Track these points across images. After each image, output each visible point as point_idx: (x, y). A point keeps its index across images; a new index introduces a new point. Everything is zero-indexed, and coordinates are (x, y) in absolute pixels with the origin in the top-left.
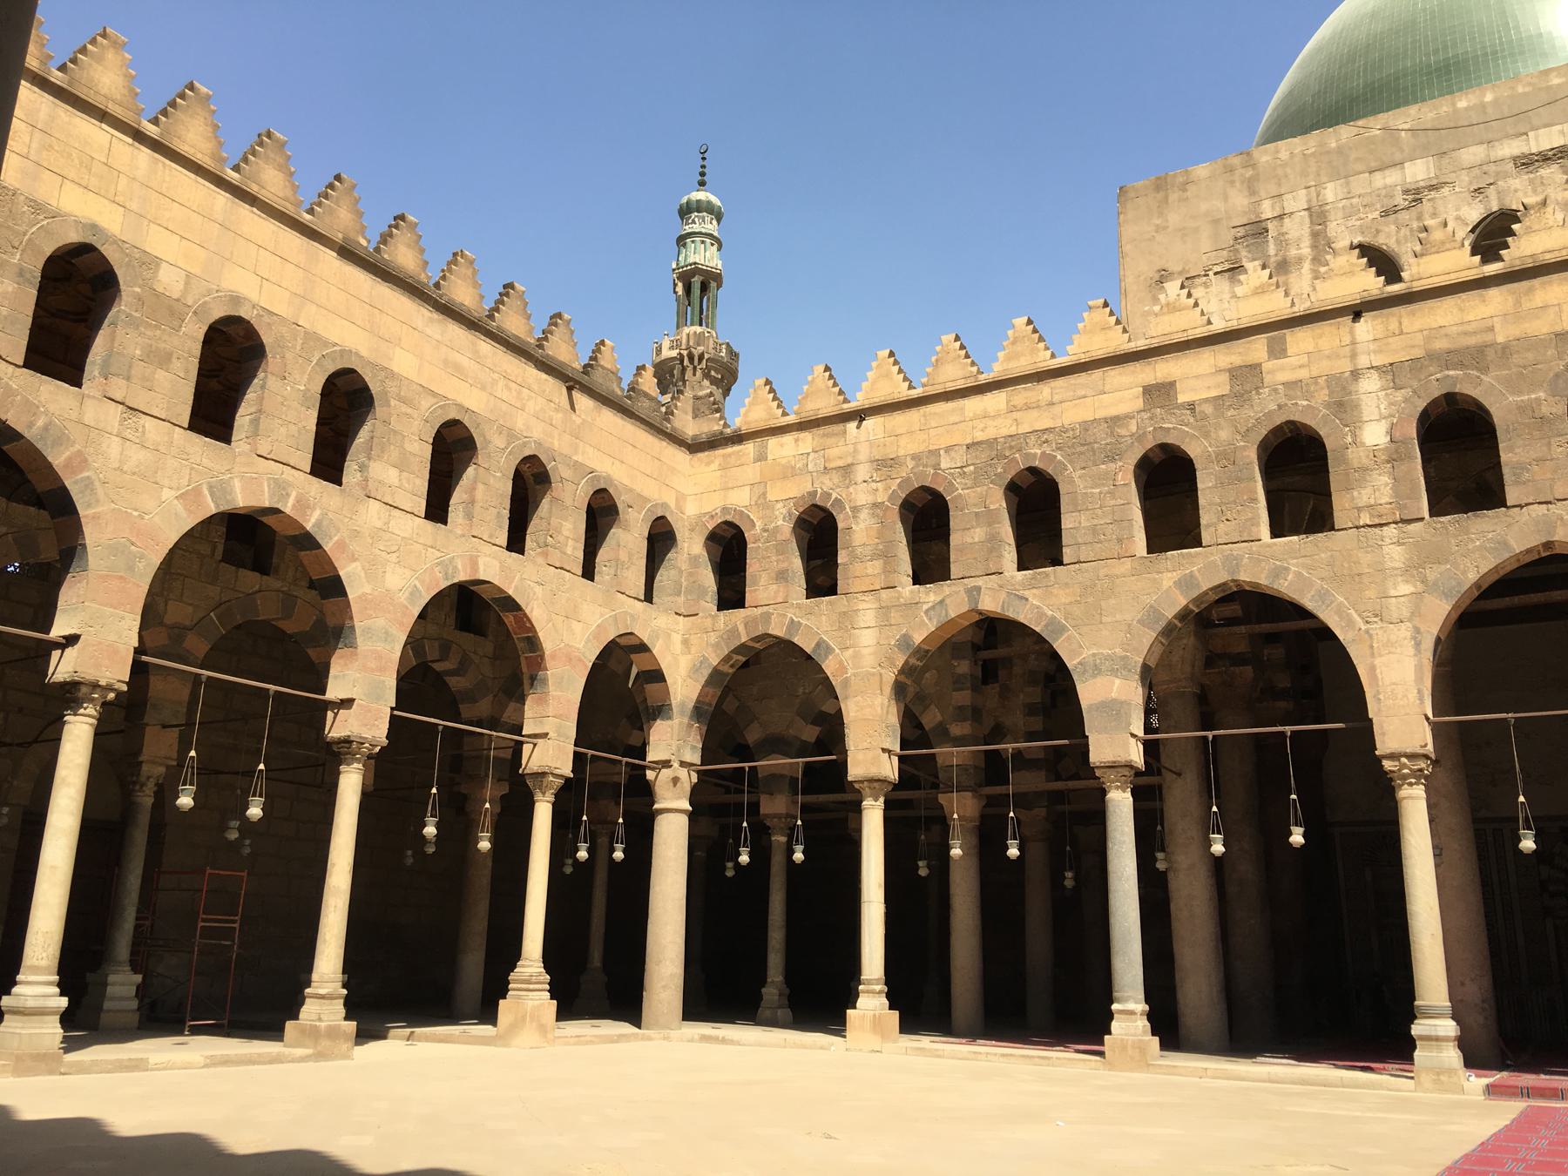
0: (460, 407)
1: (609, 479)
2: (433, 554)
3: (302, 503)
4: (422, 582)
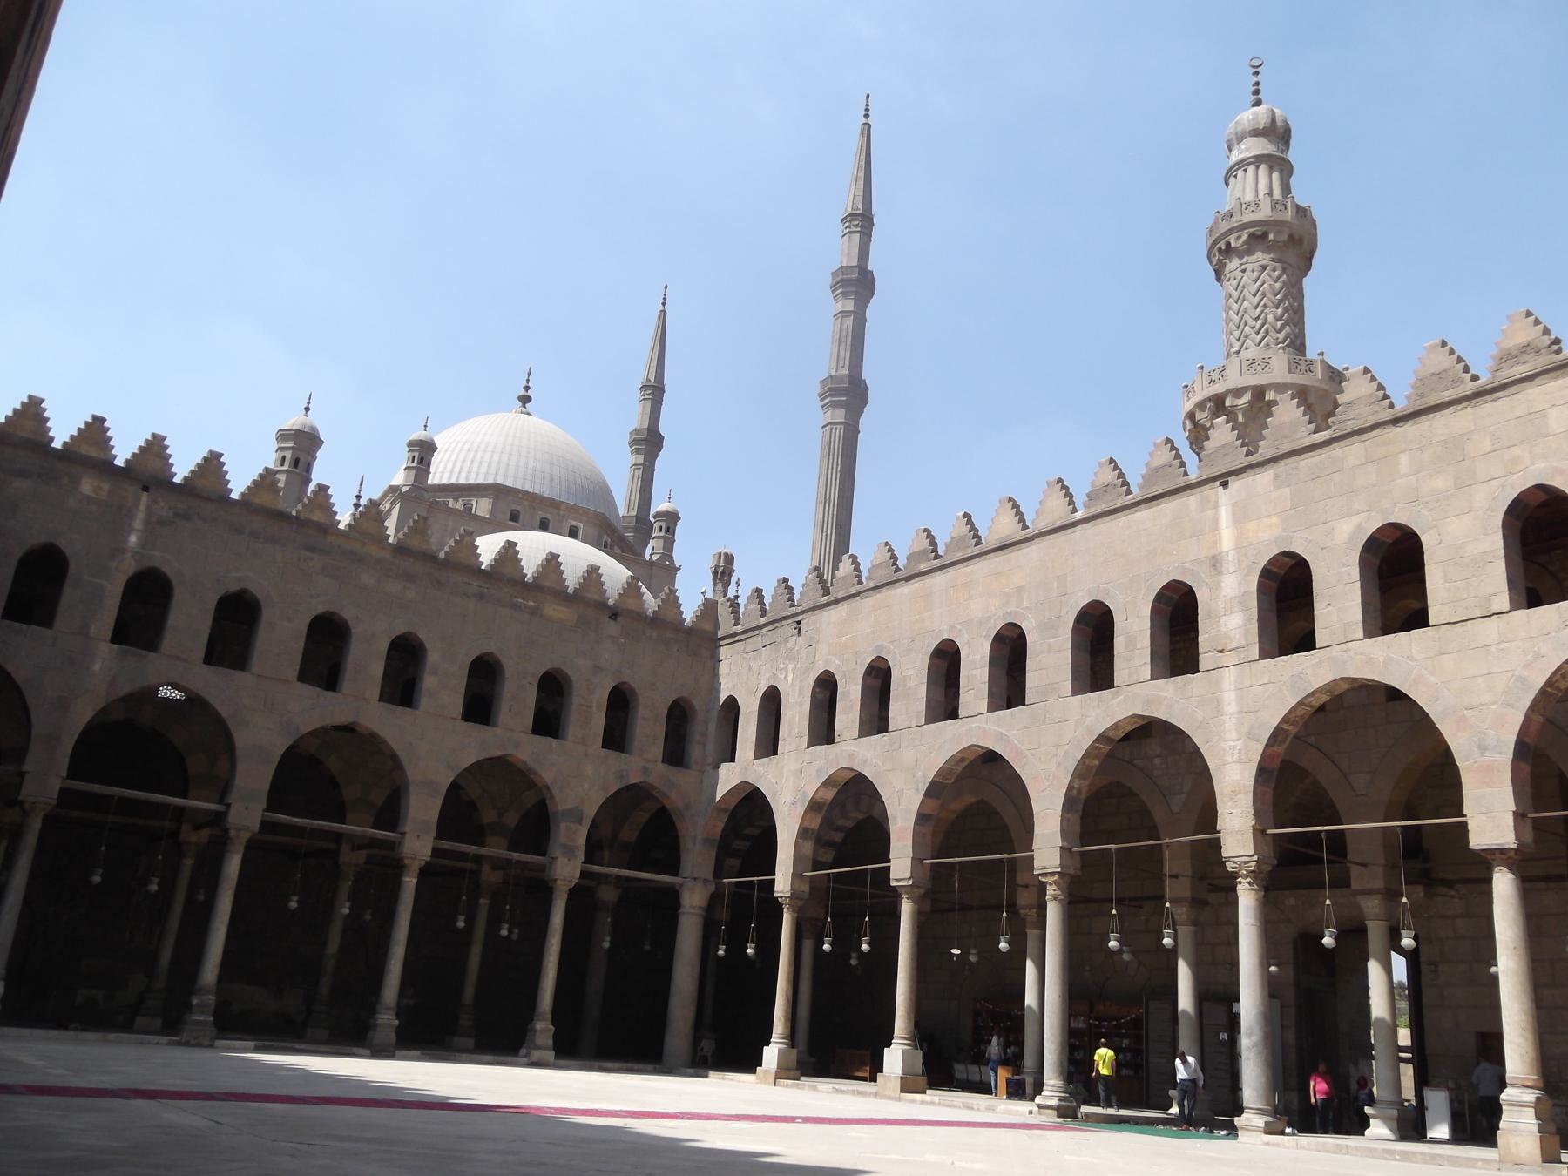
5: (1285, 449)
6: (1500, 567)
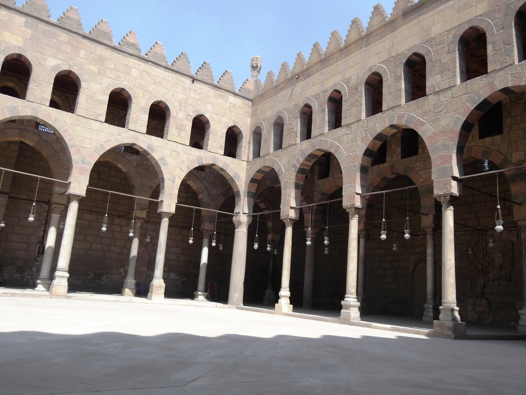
0: (467, 22)
3: (401, 117)
4: (459, 114)
5: (34, 14)
6: (106, 107)
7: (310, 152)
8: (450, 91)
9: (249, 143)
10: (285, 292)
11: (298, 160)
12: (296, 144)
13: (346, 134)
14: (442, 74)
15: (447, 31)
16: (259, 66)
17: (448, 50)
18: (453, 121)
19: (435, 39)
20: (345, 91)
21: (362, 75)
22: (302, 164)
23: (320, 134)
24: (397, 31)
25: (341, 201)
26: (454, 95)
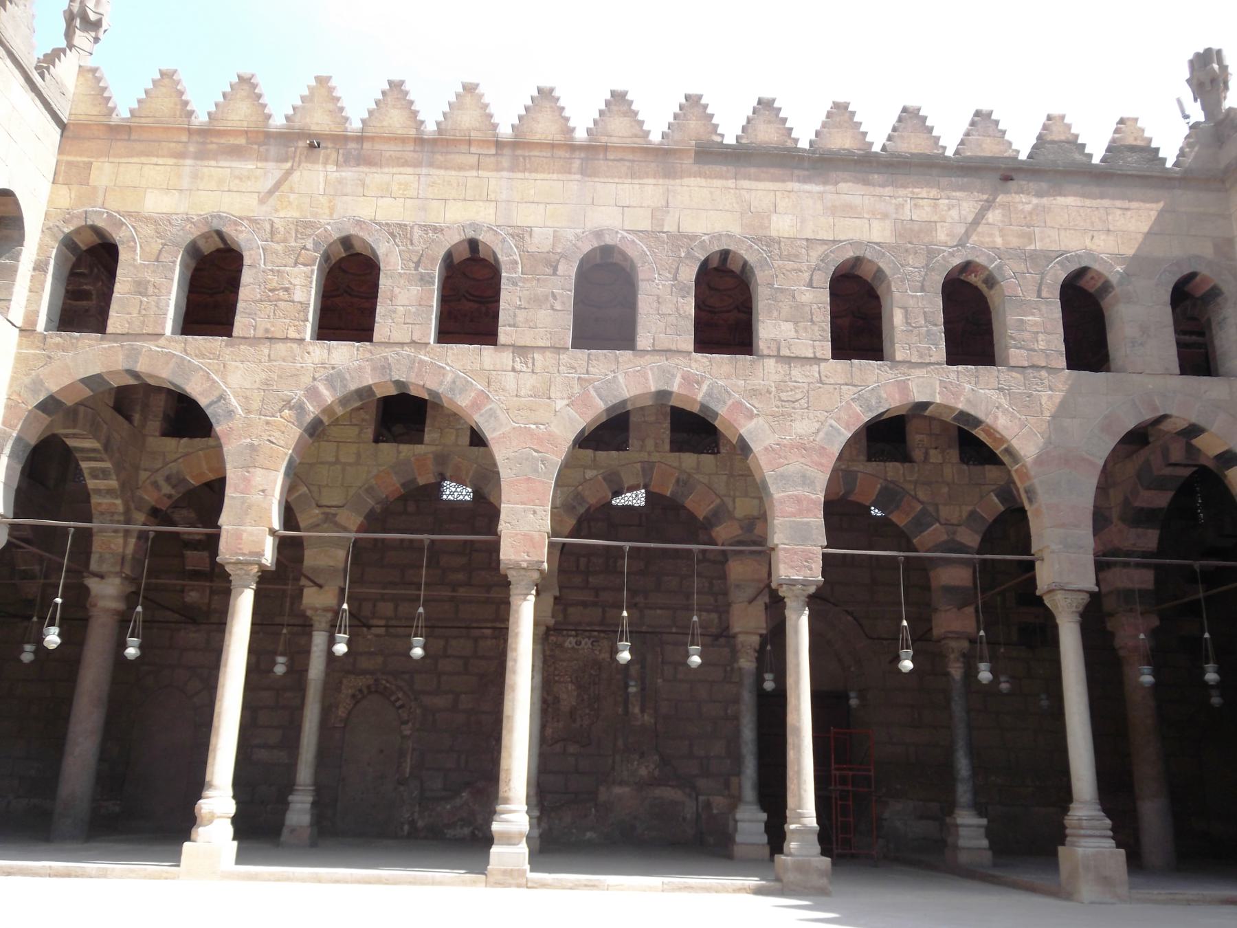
0: (852, 244)
1: (1090, 254)
2: (849, 392)
3: (688, 380)
4: (838, 420)
7: (369, 380)
8: (816, 368)
9: (40, 267)
10: (218, 801)
11: (312, 392)
12: (302, 340)
13: (514, 370)
14: (796, 323)
15: (807, 240)
16: (105, 25)
17: (811, 280)
18: (825, 429)
19: (779, 243)
20: (508, 256)
21: (572, 238)
22: (328, 410)
23: (413, 342)
24: (678, 181)
25: (495, 548)
26: (824, 378)
